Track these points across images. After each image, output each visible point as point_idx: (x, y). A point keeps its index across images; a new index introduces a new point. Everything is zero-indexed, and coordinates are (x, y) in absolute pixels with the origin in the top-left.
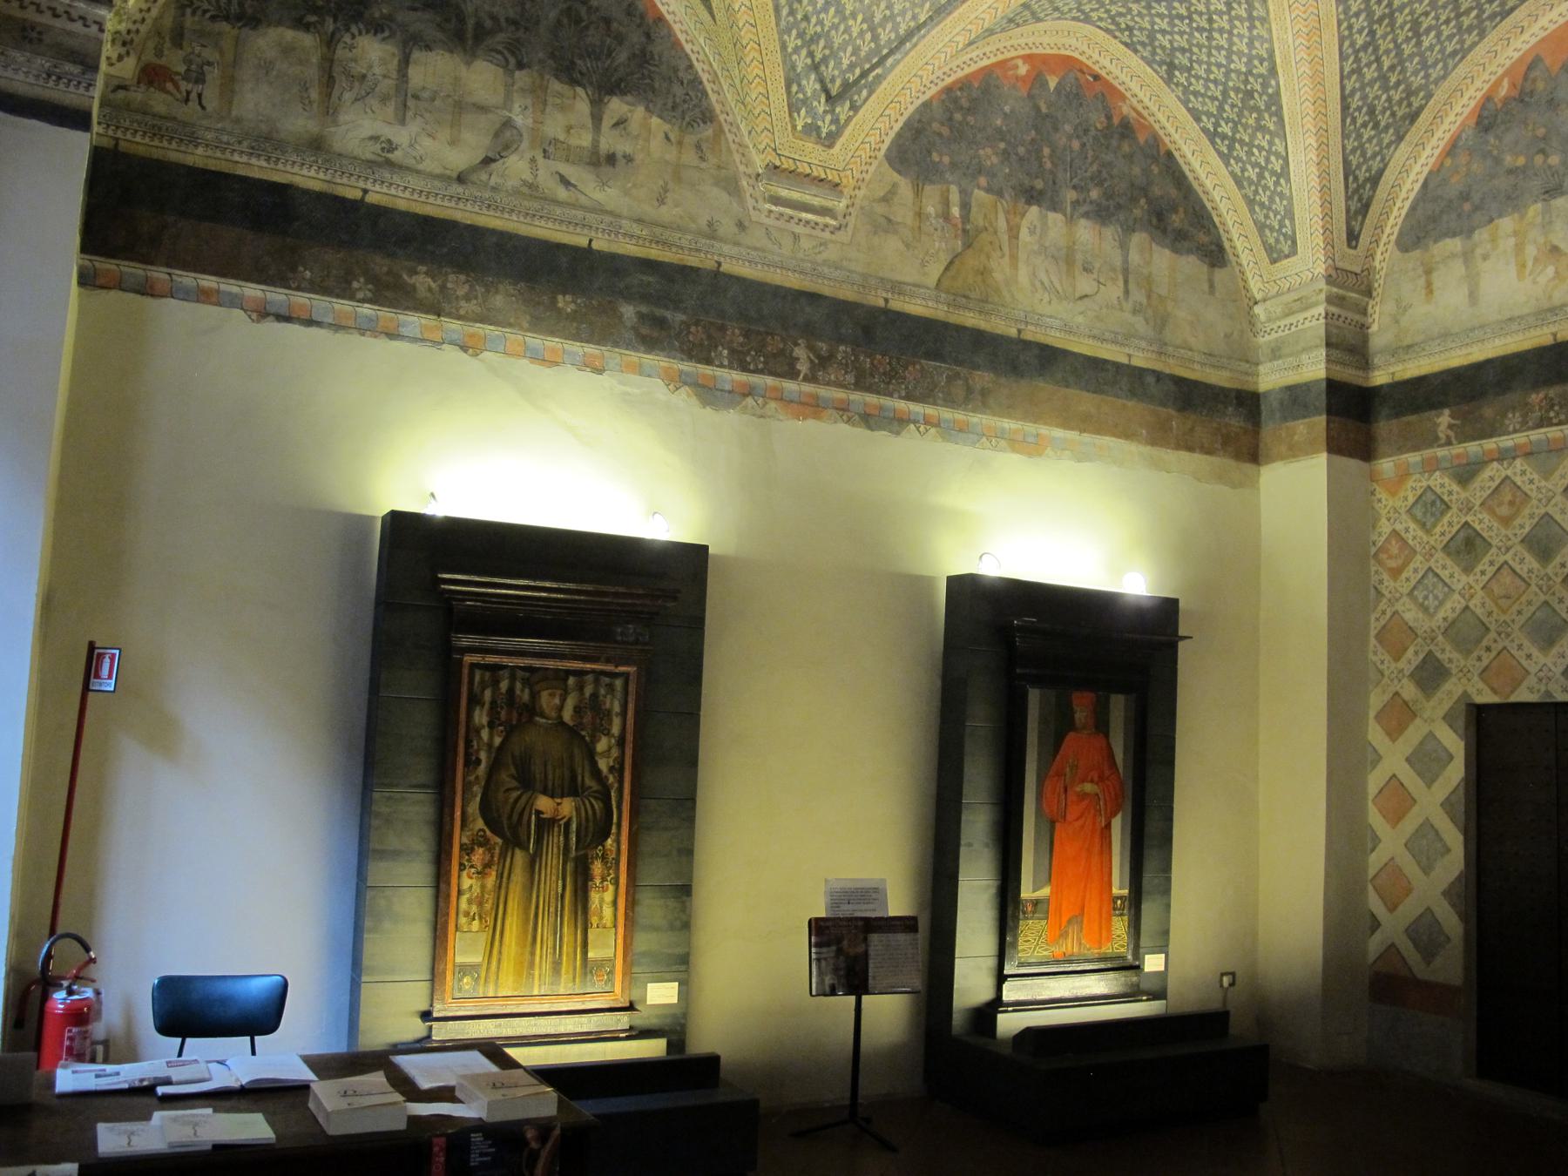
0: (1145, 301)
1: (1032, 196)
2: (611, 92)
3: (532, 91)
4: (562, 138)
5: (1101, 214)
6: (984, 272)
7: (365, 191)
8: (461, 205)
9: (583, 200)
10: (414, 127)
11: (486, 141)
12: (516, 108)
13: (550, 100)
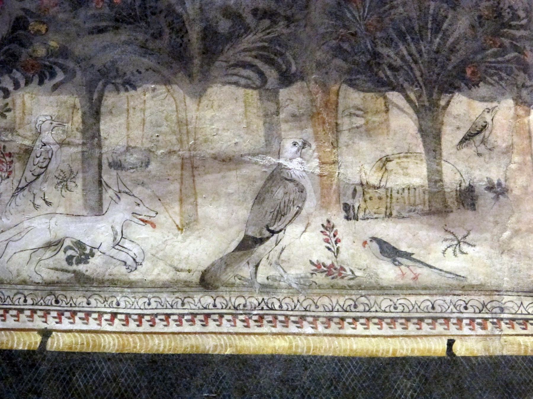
2: (451, 88)
3: (313, 116)
4: (374, 180)
7: (46, 334)
8: (212, 326)
9: (426, 276)
10: (118, 214)
11: (243, 212)
12: (289, 149)
13: (345, 123)
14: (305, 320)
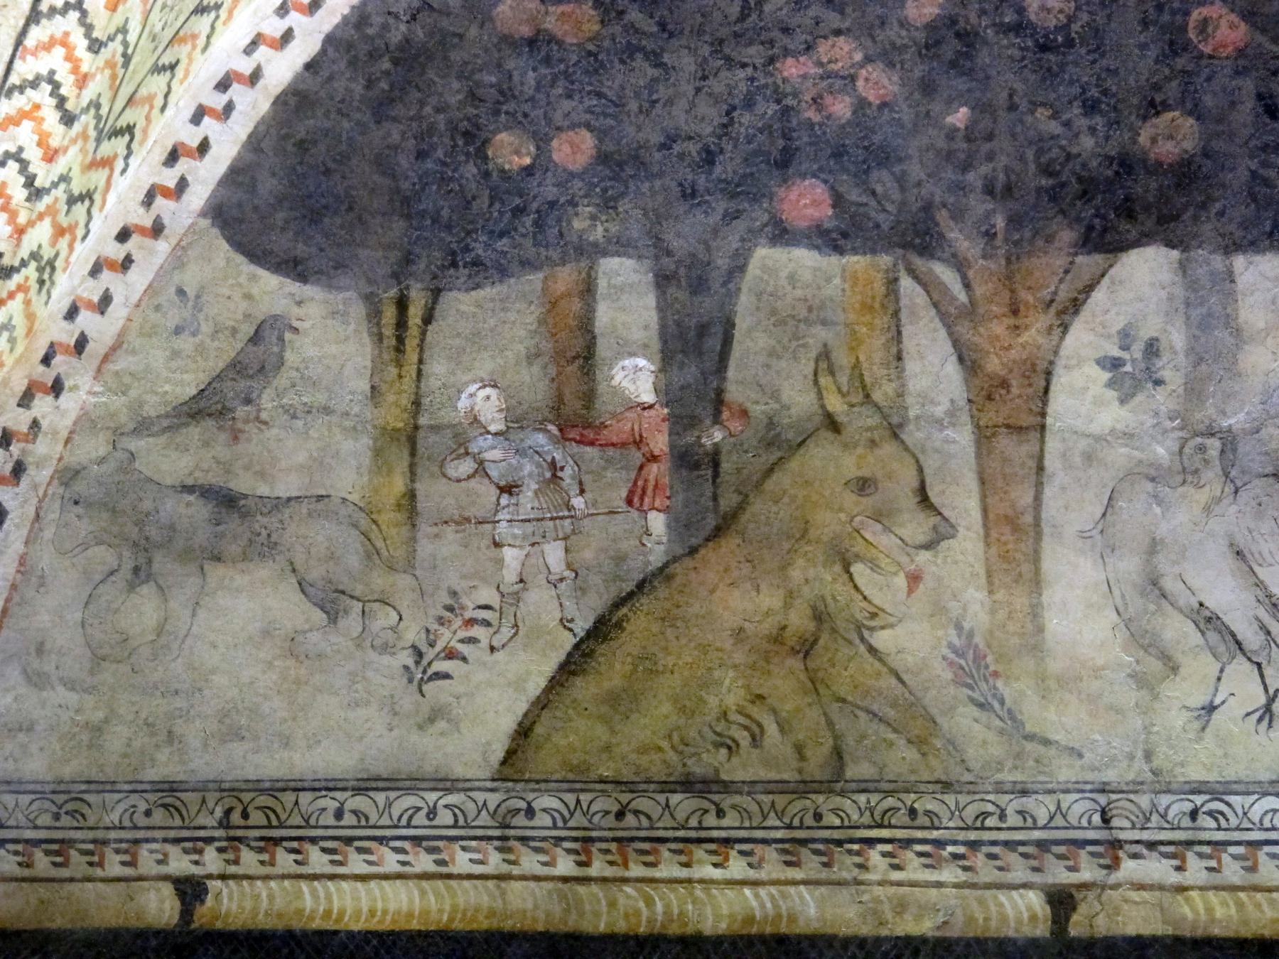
1: (1116, 207)
6: (809, 644)
14: (1049, 851)
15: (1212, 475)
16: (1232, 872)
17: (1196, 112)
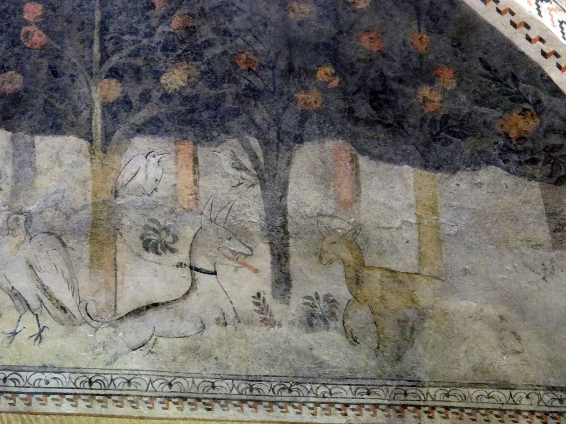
0: (342, 292)
5: (195, 120)
15: (21, 231)
16: (20, 406)
17: (22, 72)
